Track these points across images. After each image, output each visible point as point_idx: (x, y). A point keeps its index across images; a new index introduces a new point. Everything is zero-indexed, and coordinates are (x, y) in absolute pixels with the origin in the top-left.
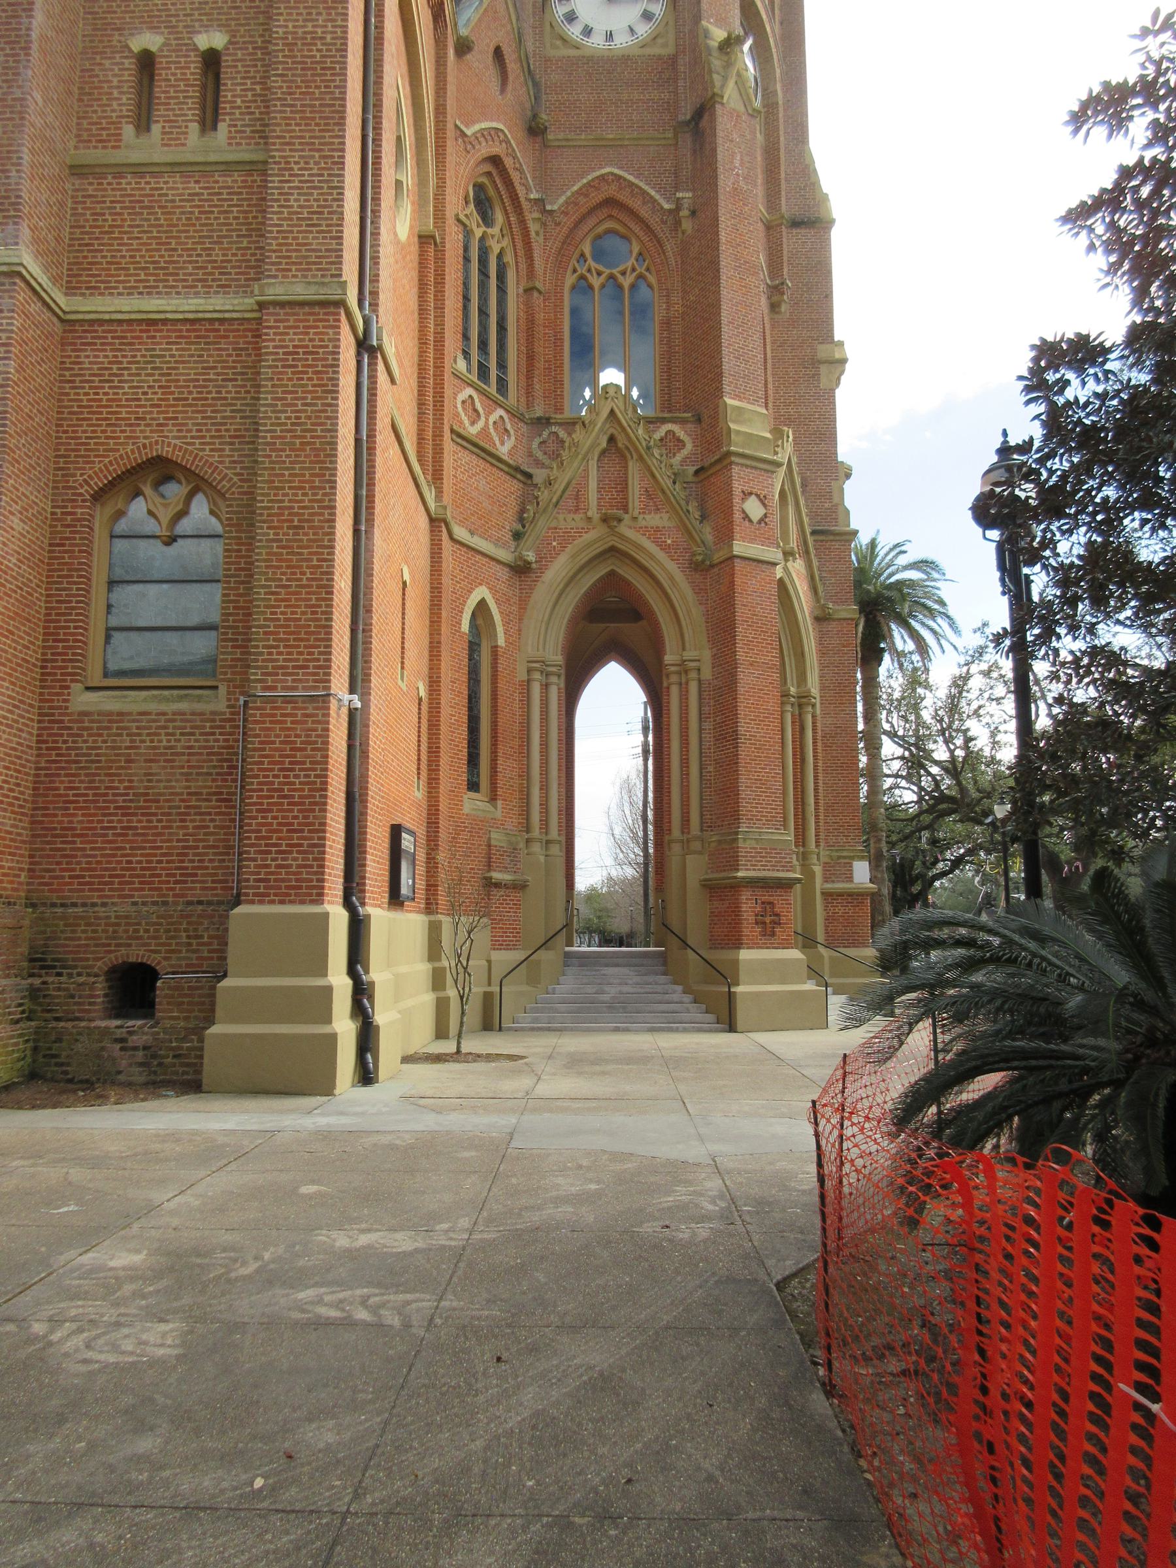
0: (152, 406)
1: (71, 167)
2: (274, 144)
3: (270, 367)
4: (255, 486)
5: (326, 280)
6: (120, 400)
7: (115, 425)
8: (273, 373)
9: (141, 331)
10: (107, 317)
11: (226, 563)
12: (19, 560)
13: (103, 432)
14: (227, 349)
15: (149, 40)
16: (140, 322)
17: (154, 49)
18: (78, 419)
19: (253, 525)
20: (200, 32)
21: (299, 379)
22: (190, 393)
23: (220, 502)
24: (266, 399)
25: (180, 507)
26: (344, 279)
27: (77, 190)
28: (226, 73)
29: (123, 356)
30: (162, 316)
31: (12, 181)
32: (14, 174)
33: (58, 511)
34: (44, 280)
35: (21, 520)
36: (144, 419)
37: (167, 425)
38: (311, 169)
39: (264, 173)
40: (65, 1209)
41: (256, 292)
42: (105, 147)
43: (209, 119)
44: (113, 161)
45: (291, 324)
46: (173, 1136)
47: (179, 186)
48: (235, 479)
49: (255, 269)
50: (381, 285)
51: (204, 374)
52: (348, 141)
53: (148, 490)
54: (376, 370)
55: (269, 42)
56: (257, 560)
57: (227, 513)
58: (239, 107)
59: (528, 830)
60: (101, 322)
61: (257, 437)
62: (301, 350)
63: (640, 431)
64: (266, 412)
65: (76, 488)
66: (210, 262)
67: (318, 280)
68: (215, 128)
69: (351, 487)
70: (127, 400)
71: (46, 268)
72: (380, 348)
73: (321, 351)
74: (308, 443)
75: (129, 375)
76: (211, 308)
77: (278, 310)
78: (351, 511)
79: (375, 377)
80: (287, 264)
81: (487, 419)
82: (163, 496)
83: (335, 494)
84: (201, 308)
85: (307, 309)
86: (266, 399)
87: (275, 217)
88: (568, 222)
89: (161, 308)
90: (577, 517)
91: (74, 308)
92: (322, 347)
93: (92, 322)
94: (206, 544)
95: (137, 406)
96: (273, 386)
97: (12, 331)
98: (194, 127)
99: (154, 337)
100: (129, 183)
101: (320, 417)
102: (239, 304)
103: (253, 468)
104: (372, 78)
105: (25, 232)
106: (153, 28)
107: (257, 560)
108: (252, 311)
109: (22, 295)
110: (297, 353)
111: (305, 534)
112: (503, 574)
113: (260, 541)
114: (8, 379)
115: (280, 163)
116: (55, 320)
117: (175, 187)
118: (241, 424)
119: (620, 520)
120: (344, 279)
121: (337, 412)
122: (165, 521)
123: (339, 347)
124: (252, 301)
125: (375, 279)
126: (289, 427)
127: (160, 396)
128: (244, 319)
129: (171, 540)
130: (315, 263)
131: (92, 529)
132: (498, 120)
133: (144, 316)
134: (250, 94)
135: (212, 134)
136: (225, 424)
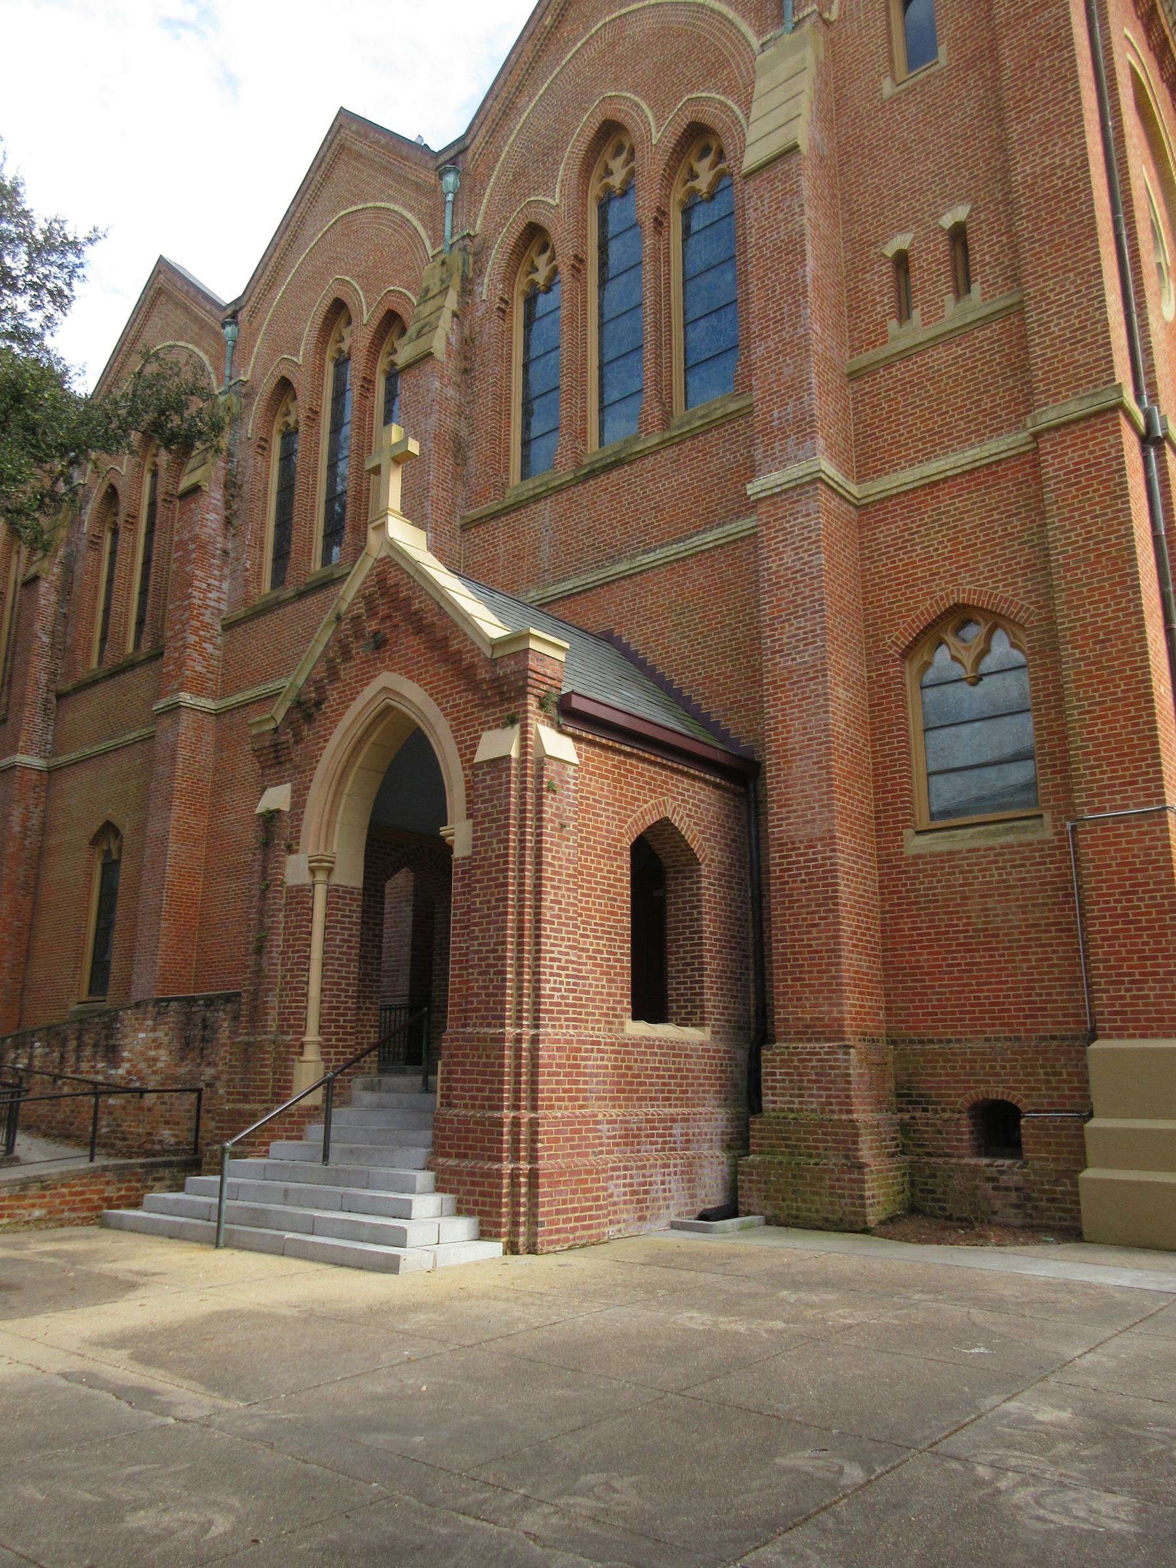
0: (944, 559)
1: (849, 375)
2: (1027, 282)
3: (1053, 491)
4: (1054, 610)
5: (1099, 390)
6: (915, 562)
7: (912, 586)
8: (1057, 496)
9: (926, 495)
10: (894, 492)
11: (1035, 691)
12: (846, 725)
13: (903, 594)
14: (1008, 487)
15: (901, 241)
16: (923, 487)
17: (905, 247)
18: (880, 589)
19: (1057, 649)
20: (943, 214)
21: (1084, 494)
22: (978, 537)
23: (1020, 633)
24: (1053, 523)
25: (982, 646)
26: (1117, 382)
27: (856, 392)
28: (972, 237)
29: (912, 522)
30: (942, 476)
31: (806, 404)
32: (806, 398)
33: (873, 674)
34: (839, 478)
35: (845, 689)
36: (938, 573)
37: (960, 573)
38: (1068, 290)
39: (1022, 312)
40: (976, 1350)
41: (1029, 425)
42: (874, 347)
43: (962, 287)
44: (882, 356)
45: (1068, 443)
46: (1067, 1286)
47: (943, 354)
48: (1032, 608)
49: (1025, 403)
50: (1158, 374)
51: (989, 516)
52: (1102, 249)
53: (949, 638)
54: (1166, 461)
55: (1010, 192)
56: (1066, 683)
57: (1029, 642)
58: (989, 263)
60: (889, 498)
61: (1049, 561)
62: (1082, 466)
64: (1055, 535)
65: (885, 651)
66: (980, 412)
67: (1091, 392)
68: (969, 291)
69: (1155, 586)
70: (920, 560)
71: (839, 467)
72: (1167, 437)
73: (1103, 460)
74: (1104, 554)
75: (920, 537)
76: (986, 454)
77: (1053, 434)
78: (1159, 612)
79: (1166, 467)
80: (1056, 388)
82: (964, 640)
83: (1140, 598)
84: (977, 457)
85: (1083, 424)
86: (1053, 523)
87: (1037, 348)
89: (940, 469)
91: (866, 493)
92: (1104, 455)
93: (882, 501)
94: (1010, 677)
95: (930, 564)
96: (1058, 508)
97: (819, 529)
98: (950, 297)
99: (938, 497)
100: (898, 370)
101: (1112, 525)
102: (1013, 441)
103: (1048, 593)
104: (1117, 178)
105: (821, 443)
106: (903, 230)
107: (1066, 683)
108: (1027, 443)
109: (824, 495)
110: (1079, 469)
111: (1113, 646)
113: (1067, 662)
114: (821, 570)
115: (1035, 297)
116: (851, 508)
117: (939, 357)
118: (1030, 553)
120: (1117, 382)
121: (1130, 514)
122: (969, 664)
123: (1122, 450)
124: (1025, 434)
125: (1151, 369)
126: (1081, 543)
127: (950, 549)
128: (1020, 454)
129: (977, 680)
130: (1084, 377)
131: (904, 685)
133: (927, 481)
134: (996, 247)
135: (967, 297)
136: (1015, 558)
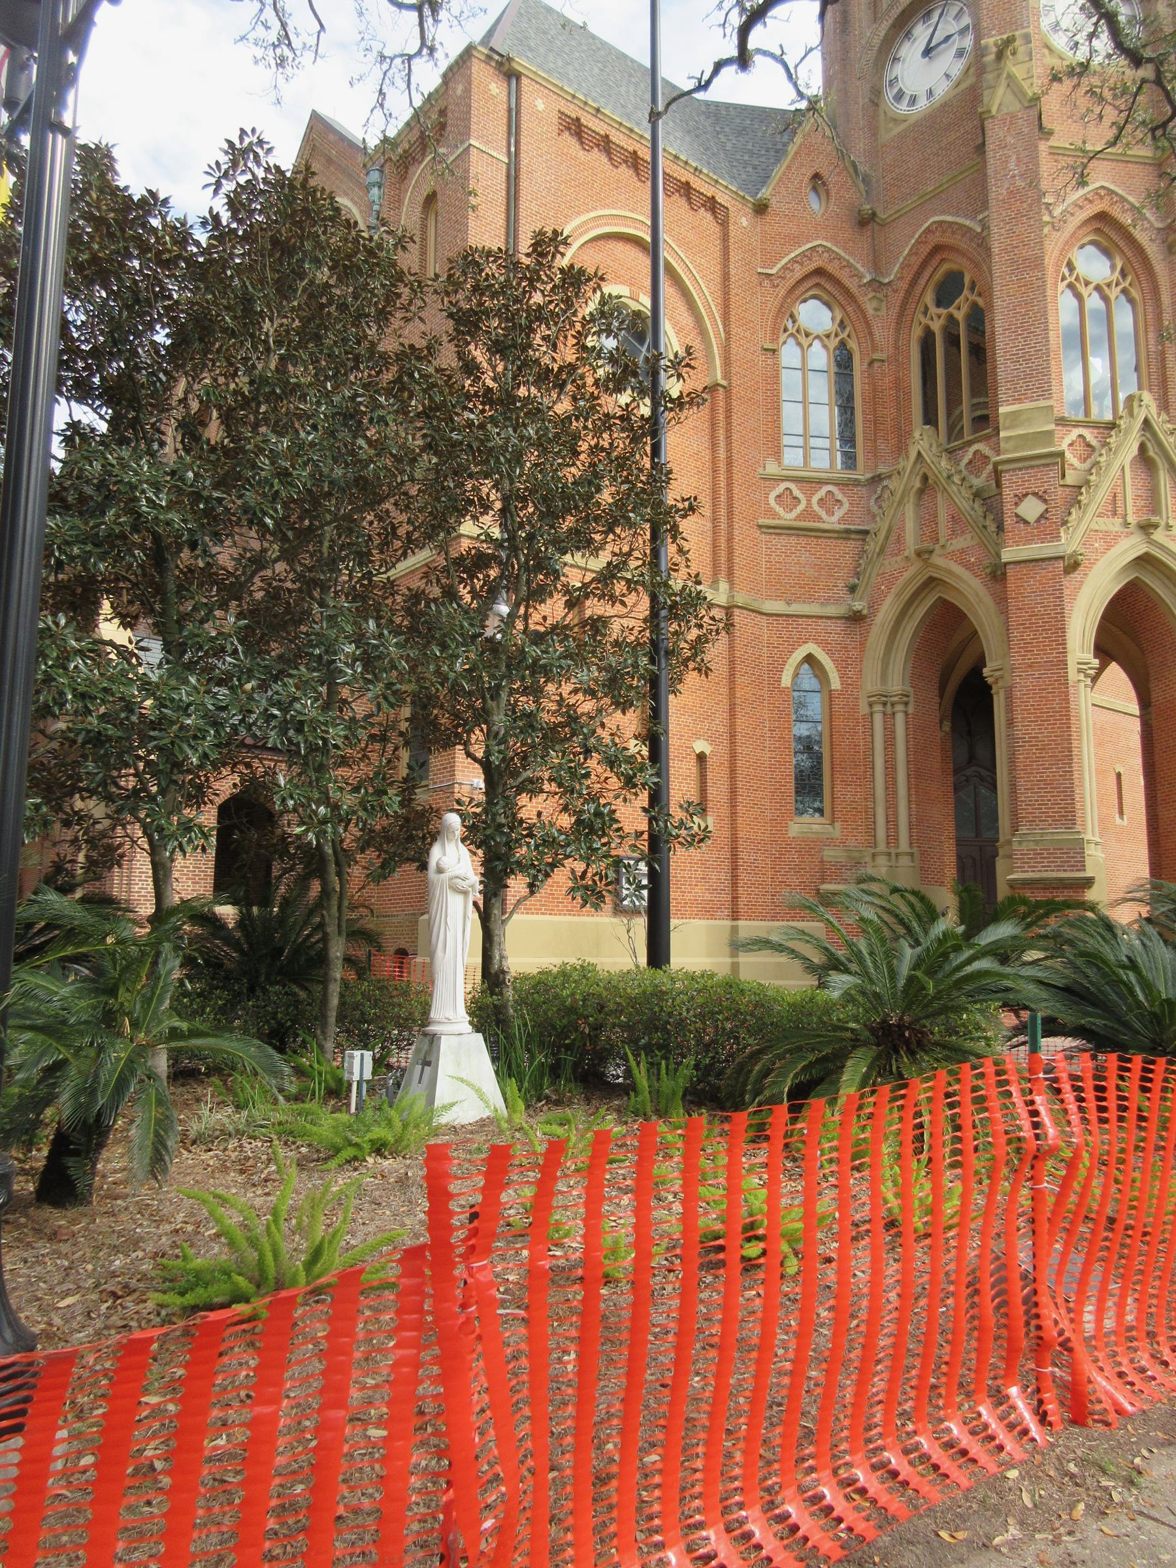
59: (875, 845)
63: (943, 463)
81: (809, 501)
88: (903, 285)
90: (899, 558)
112: (839, 626)
119: (931, 552)
132: (817, 238)
